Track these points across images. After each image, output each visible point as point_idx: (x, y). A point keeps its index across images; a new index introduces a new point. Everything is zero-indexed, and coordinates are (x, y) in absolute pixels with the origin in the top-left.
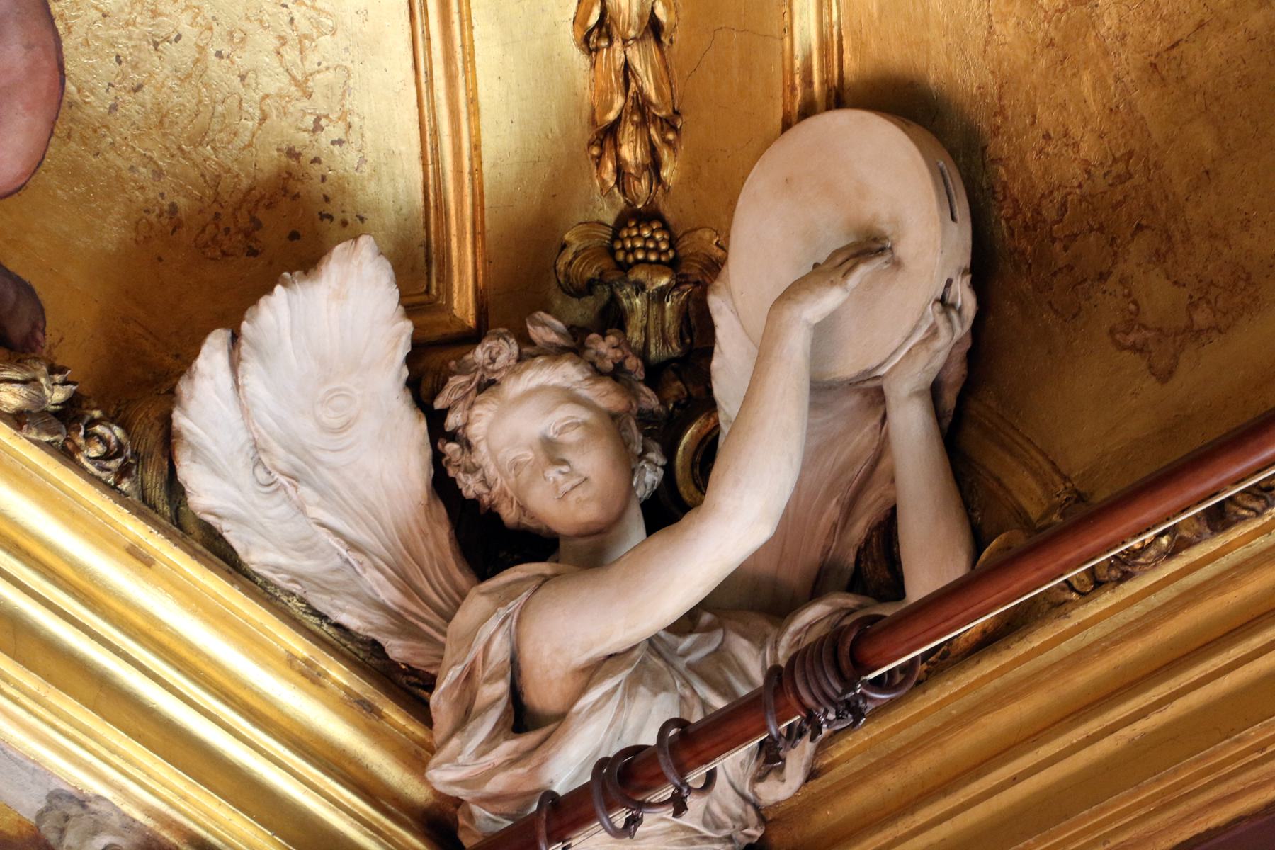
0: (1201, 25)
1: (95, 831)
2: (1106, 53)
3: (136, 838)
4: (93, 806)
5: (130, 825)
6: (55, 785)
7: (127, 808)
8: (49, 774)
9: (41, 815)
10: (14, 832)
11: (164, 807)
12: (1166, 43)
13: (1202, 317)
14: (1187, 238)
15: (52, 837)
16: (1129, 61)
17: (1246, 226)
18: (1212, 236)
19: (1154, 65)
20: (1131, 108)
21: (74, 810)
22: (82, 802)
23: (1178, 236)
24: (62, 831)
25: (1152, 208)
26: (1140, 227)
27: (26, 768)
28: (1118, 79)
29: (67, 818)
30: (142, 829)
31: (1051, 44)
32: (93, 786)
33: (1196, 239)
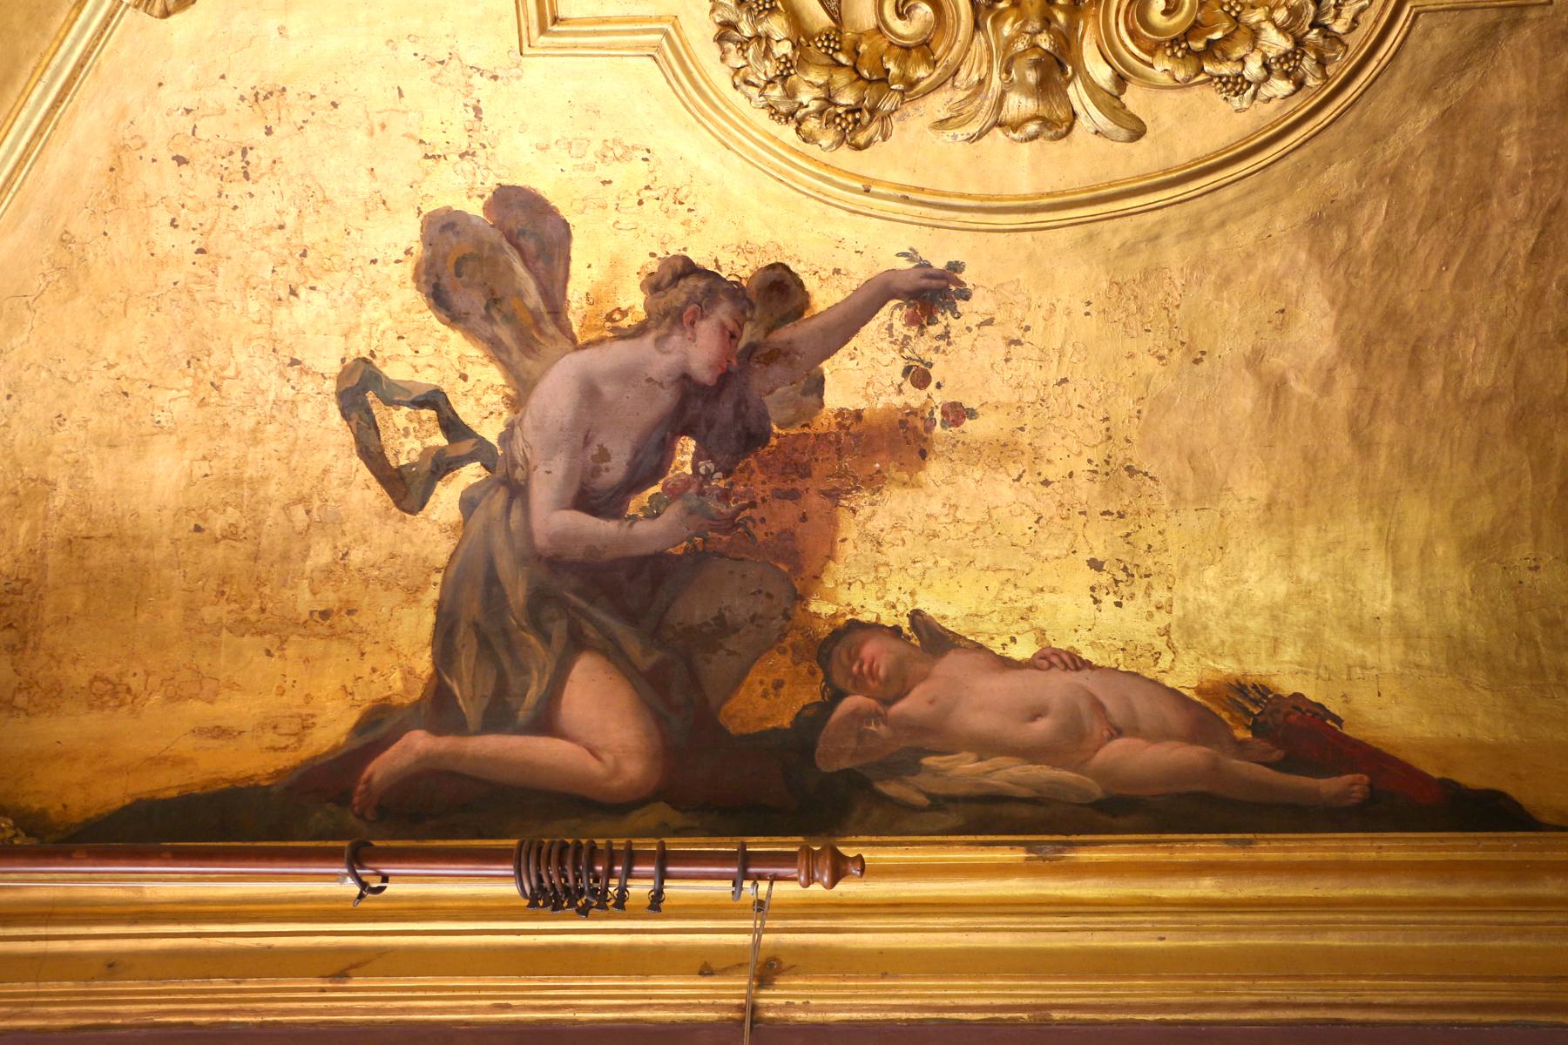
0: (109, 536)
2: (46, 518)
12: (84, 534)
13: (21, 700)
14: (36, 648)
16: (57, 531)
17: (75, 661)
18: (52, 656)
19: (70, 542)
20: (43, 556)
23: (31, 644)
25: (25, 619)
26: (10, 626)
28: (45, 536)
31: (16, 494)
33: (41, 653)
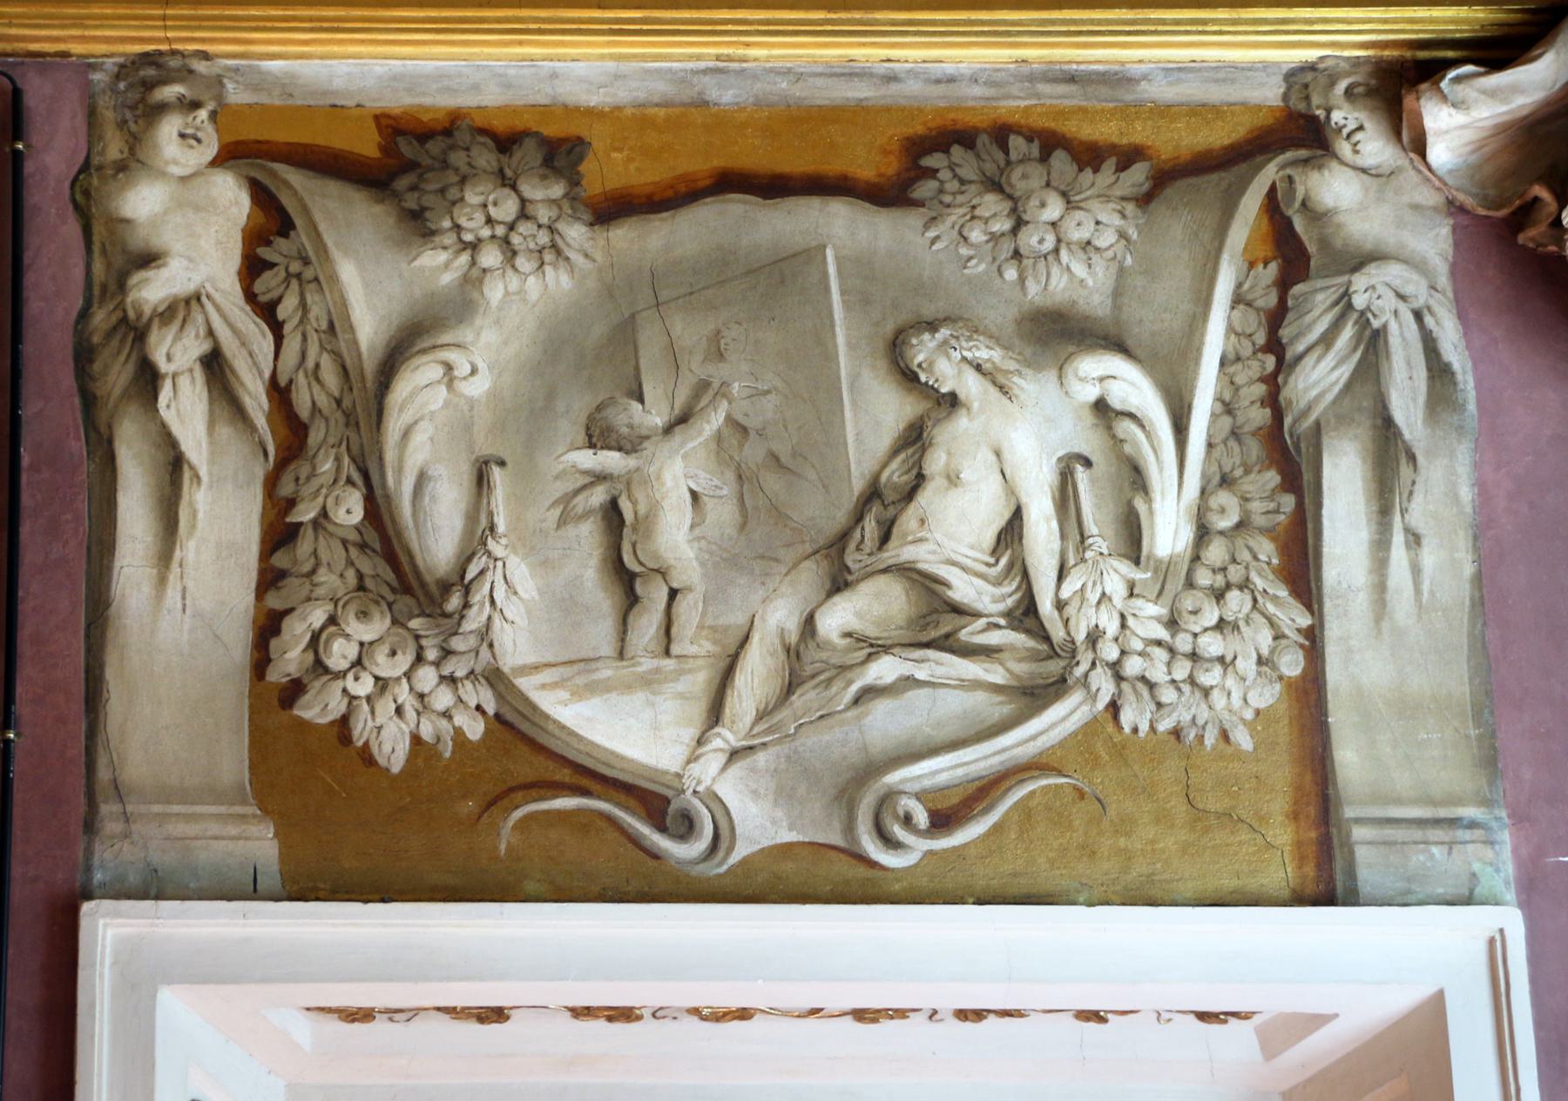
1: (1332, 83)
3: (1368, 68)
4: (1321, 66)
5: (1356, 62)
6: (1285, 69)
7: (1346, 53)
8: (1277, 64)
9: (1285, 97)
10: (1271, 121)
11: (1373, 37)
15: (1301, 107)
21: (1309, 77)
22: (1311, 67)
24: (1307, 98)
27: (1257, 70)
29: (1306, 86)
30: (1367, 59)
32: (1311, 55)
